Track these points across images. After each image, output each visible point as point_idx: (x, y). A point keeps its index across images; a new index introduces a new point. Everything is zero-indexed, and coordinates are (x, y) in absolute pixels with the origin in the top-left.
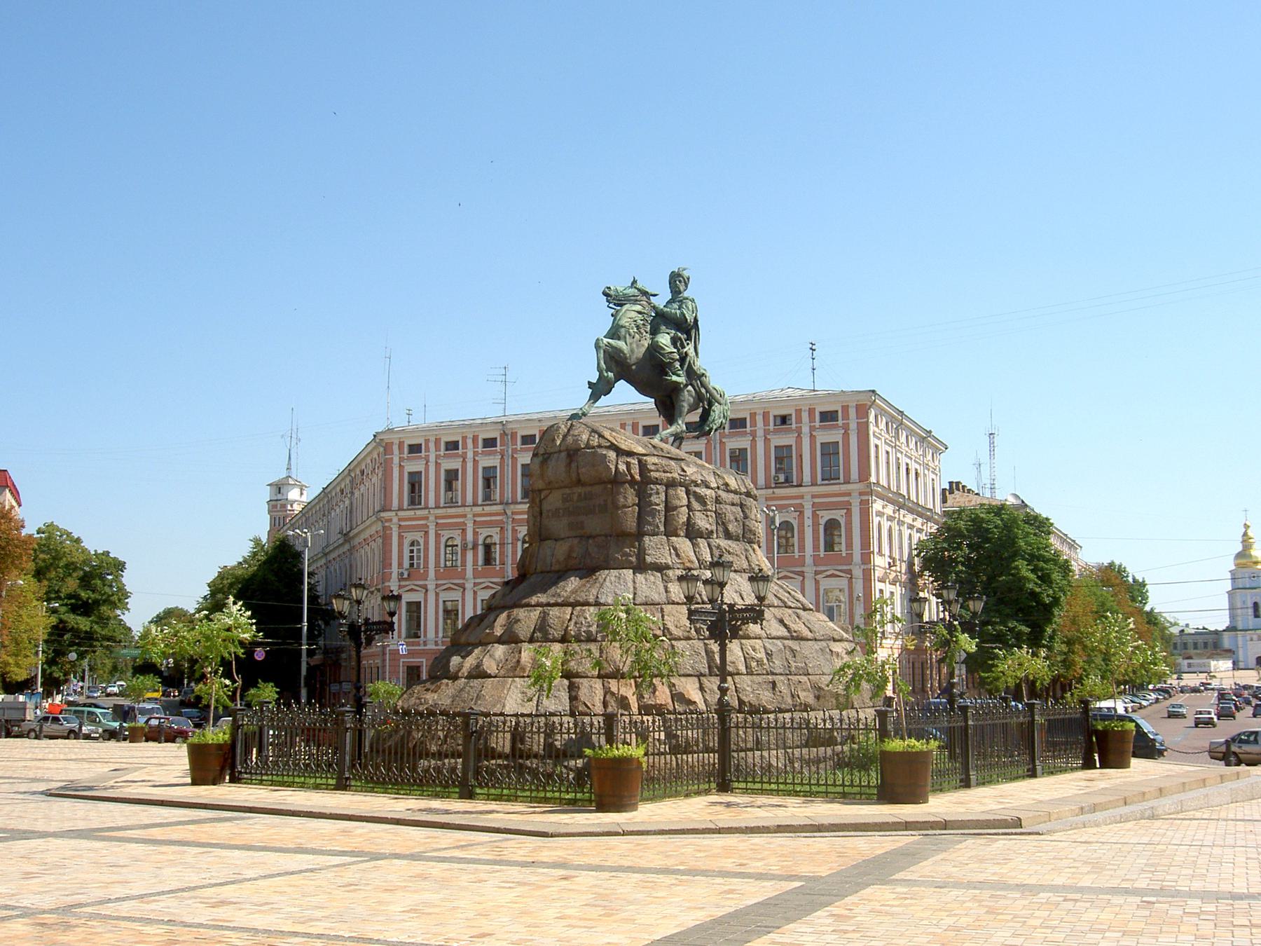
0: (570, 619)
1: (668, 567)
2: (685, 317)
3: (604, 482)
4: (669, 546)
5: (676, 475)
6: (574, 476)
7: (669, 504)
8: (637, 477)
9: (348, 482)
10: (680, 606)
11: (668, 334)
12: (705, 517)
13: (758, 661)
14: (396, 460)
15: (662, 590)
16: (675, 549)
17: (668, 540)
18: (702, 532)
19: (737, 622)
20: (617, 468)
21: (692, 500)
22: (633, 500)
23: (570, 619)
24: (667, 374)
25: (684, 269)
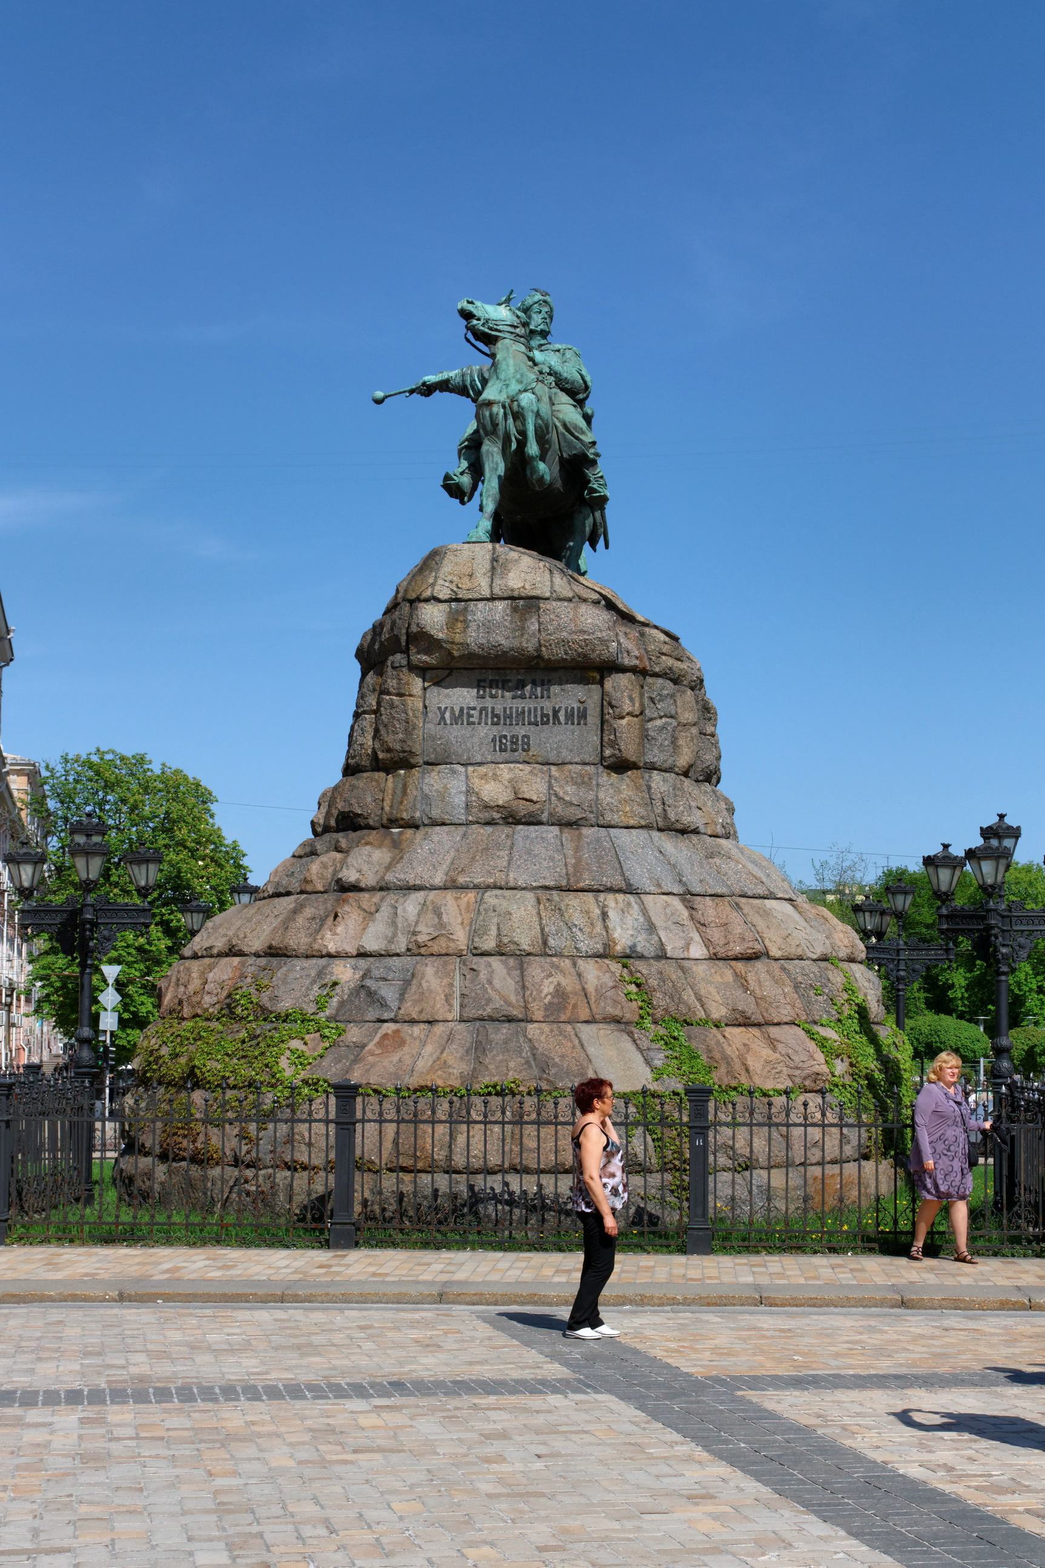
1: (696, 831)
2: (585, 382)
5: (683, 666)
6: (530, 646)
20: (619, 643)
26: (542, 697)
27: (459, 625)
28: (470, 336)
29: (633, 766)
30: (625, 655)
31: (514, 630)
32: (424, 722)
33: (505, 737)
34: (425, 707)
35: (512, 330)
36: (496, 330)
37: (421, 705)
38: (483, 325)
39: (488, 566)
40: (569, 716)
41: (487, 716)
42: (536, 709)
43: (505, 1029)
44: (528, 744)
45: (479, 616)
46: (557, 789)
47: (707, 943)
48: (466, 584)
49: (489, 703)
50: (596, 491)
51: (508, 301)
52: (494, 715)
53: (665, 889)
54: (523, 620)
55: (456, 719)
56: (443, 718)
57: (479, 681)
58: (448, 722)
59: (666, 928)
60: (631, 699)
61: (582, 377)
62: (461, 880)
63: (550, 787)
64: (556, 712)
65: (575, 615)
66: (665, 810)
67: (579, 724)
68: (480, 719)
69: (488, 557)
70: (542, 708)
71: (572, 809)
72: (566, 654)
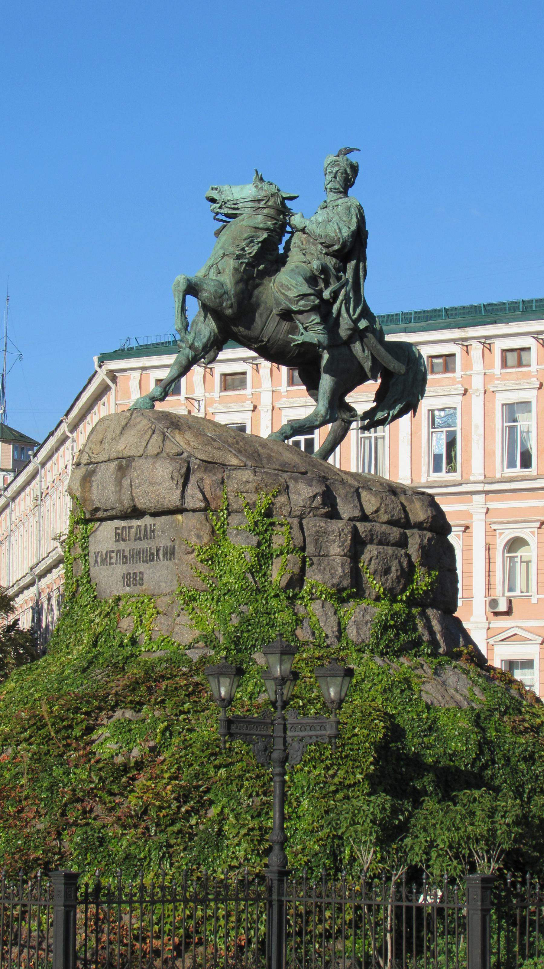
25: (349, 151)
26: (151, 538)
27: (88, 485)
30: (190, 499)
31: (116, 486)
33: (130, 574)
35: (251, 204)
38: (220, 208)
39: (118, 431)
40: (165, 554)
44: (142, 579)
49: (122, 545)
50: (294, 340)
52: (125, 557)
54: (124, 475)
55: (104, 561)
56: (96, 561)
58: (99, 564)
60: (199, 537)
64: (158, 551)
65: (153, 469)
67: (170, 559)
68: (117, 560)
69: (123, 423)
70: (150, 548)
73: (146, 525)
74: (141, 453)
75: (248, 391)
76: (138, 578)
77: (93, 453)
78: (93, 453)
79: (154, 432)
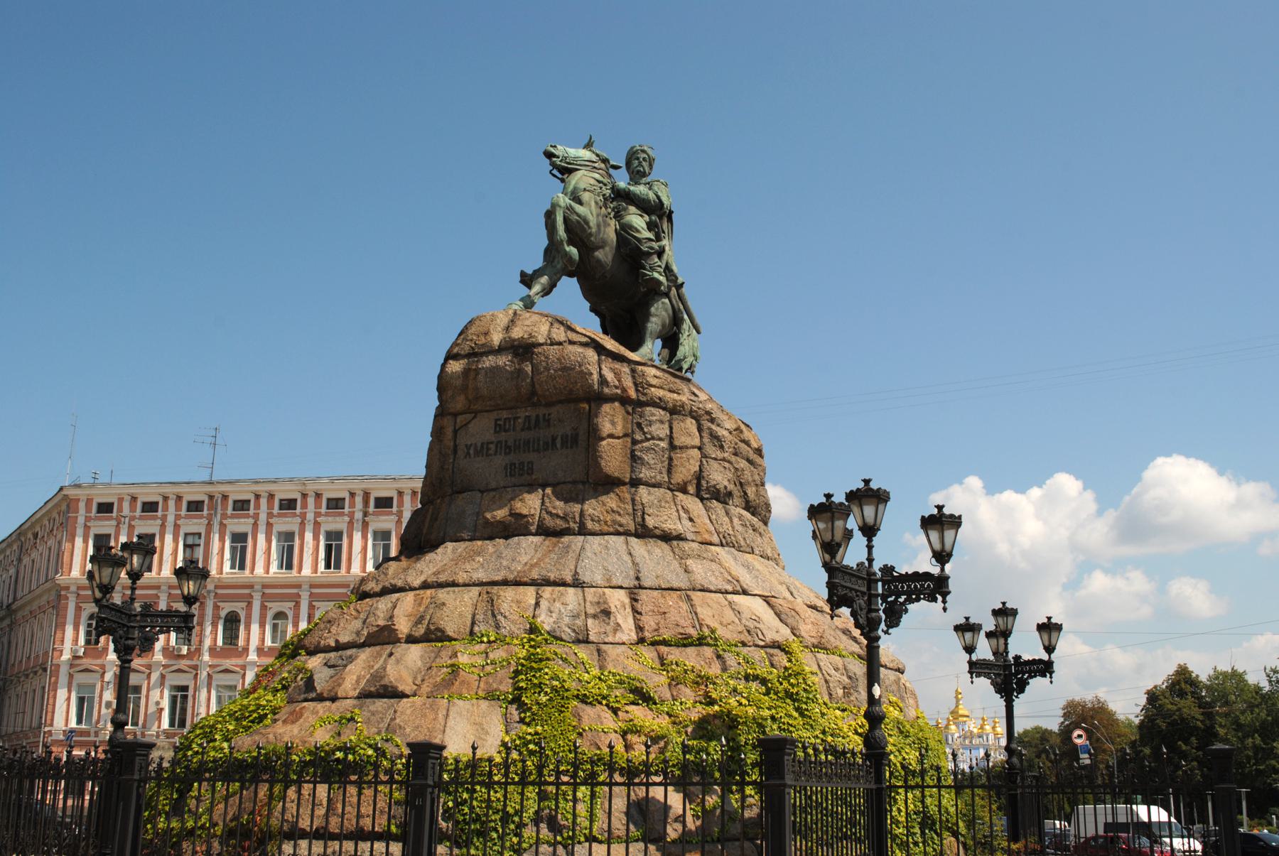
0: (537, 604)
1: (680, 538)
3: (578, 400)
4: (676, 505)
5: (684, 399)
7: (677, 443)
8: (632, 394)
9: (15, 547)
10: (713, 595)
11: (641, 216)
12: (723, 469)
13: (844, 688)
14: (81, 520)
15: (681, 571)
16: (686, 511)
17: (674, 495)
18: (718, 491)
19: (898, 596)
20: (601, 375)
21: (706, 440)
22: (624, 427)
23: (537, 604)
24: (645, 269)
28: (555, 172)
29: (618, 483)
32: (454, 460)
33: (515, 464)
34: (455, 446)
35: (587, 163)
36: (573, 164)
37: (452, 444)
40: (564, 444)
41: (501, 448)
42: (539, 440)
43: (380, 704)
44: (532, 469)
45: (487, 364)
46: (548, 505)
47: (639, 628)
48: (482, 340)
49: (503, 436)
51: (588, 146)
52: (509, 447)
53: (614, 582)
55: (477, 453)
56: (468, 453)
57: (496, 420)
58: (472, 456)
59: (595, 616)
60: (613, 423)
61: (658, 197)
62: (432, 579)
63: (543, 503)
64: (554, 439)
66: (643, 519)
68: (496, 451)
71: (559, 522)
72: (555, 388)
73: (537, 416)
74: (544, 341)
75: (160, 513)
76: (526, 468)
77: (475, 344)
78: (475, 344)
79: (552, 324)
